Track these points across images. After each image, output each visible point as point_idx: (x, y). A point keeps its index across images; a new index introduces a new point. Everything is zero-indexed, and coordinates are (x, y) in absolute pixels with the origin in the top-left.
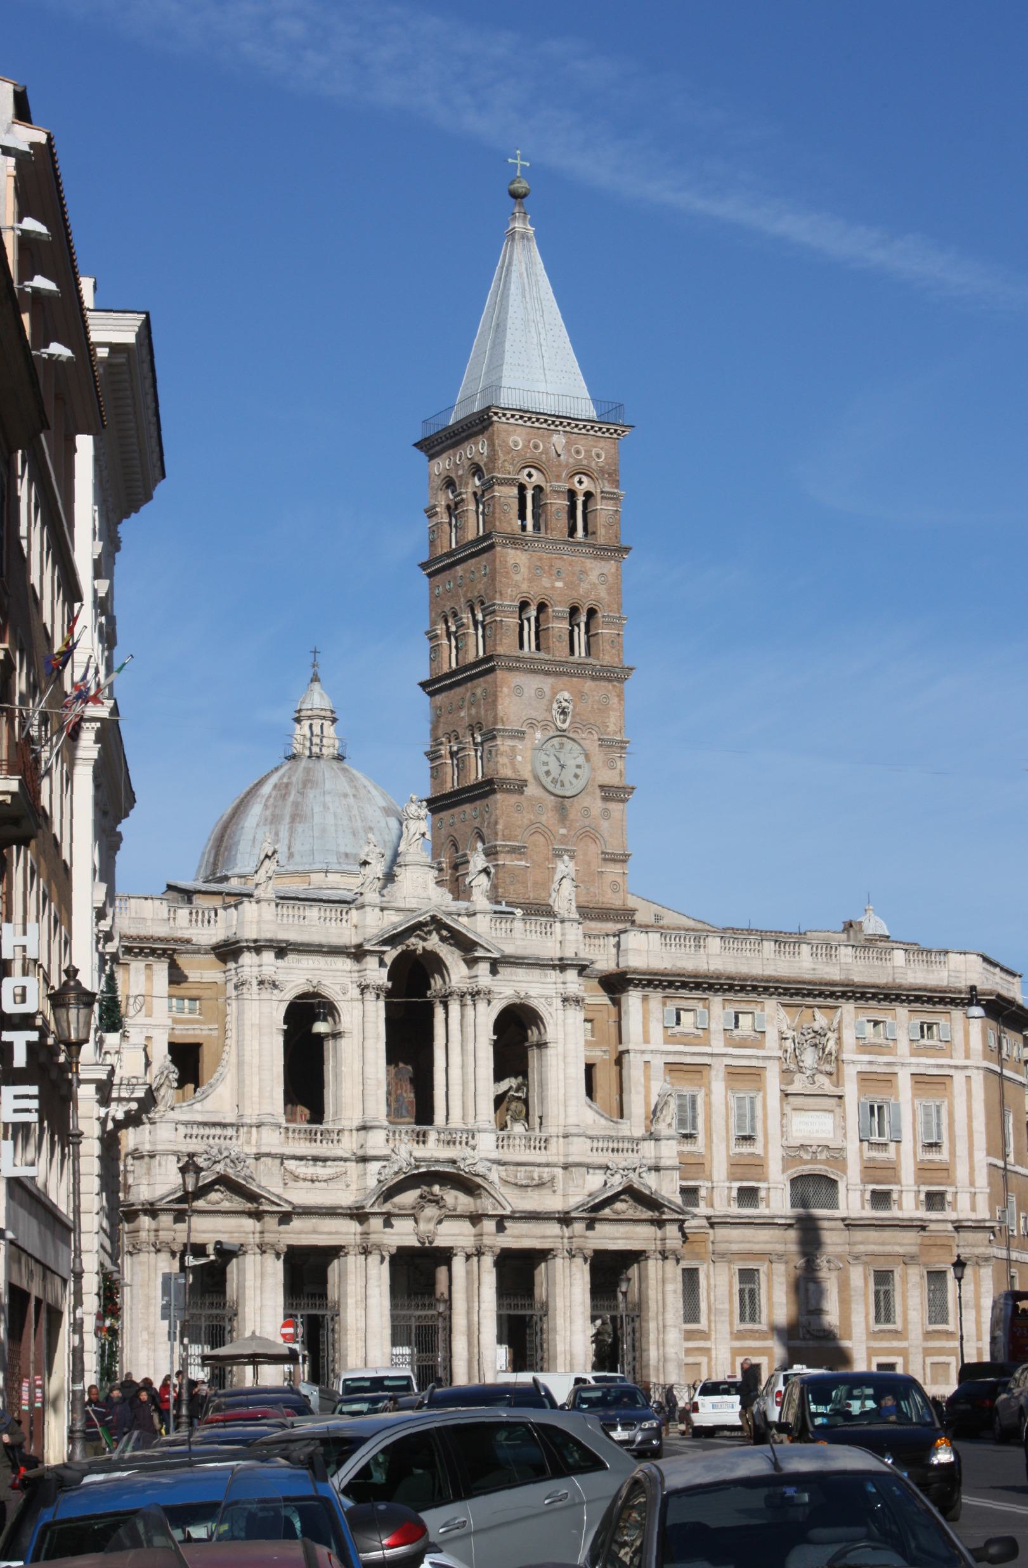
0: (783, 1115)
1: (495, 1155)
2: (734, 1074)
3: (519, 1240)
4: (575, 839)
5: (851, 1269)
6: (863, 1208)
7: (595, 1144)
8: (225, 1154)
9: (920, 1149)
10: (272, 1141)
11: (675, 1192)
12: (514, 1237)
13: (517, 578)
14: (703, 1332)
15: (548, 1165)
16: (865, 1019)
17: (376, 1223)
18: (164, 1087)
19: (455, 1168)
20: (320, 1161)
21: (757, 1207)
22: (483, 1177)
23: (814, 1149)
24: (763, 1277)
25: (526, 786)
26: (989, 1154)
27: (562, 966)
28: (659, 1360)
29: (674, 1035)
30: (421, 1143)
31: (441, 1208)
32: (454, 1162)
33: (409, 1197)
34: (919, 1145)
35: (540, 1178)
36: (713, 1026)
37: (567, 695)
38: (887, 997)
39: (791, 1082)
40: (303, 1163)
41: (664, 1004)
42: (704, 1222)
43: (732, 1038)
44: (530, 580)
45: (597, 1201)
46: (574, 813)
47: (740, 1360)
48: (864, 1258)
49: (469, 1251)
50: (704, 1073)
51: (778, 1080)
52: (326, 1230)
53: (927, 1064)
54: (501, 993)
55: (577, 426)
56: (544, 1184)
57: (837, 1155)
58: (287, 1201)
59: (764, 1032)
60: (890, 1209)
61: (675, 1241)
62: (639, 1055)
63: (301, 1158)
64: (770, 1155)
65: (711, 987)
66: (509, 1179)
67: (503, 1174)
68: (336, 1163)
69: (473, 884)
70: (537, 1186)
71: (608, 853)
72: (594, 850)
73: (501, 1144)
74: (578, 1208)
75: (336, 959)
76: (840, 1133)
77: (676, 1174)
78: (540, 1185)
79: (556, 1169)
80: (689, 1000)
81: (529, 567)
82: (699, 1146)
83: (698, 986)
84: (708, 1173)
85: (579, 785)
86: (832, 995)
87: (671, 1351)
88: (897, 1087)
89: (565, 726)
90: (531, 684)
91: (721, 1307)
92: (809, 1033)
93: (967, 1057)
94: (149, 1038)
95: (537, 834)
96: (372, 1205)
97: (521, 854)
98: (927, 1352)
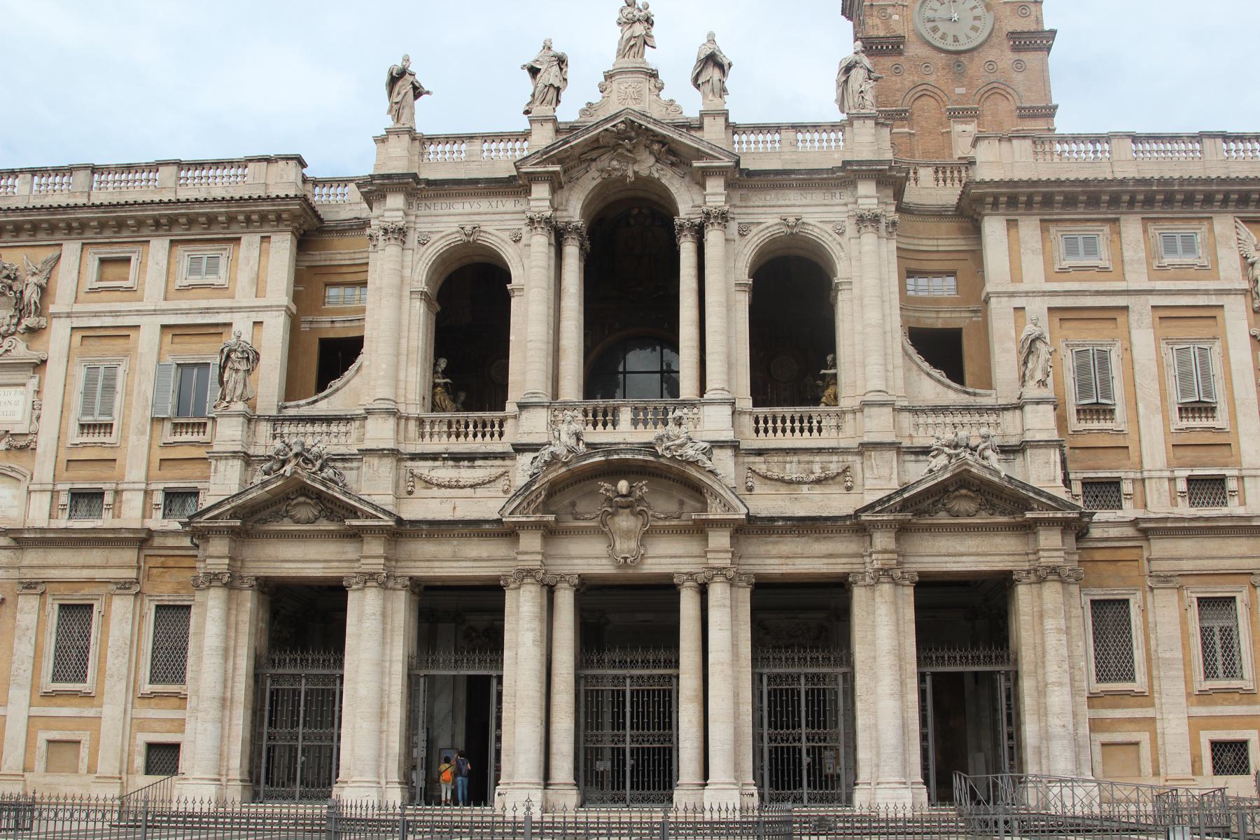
1: (728, 435)
2: (1166, 316)
3: (788, 561)
4: (977, 97)
7: (922, 419)
8: (296, 449)
10: (380, 433)
14: (1141, 694)
15: (833, 451)
17: (531, 542)
18: (227, 370)
19: (651, 454)
20: (464, 459)
21: (1224, 504)
22: (694, 463)
24: (1239, 605)
25: (903, 43)
28: (1041, 739)
29: (1063, 271)
30: (609, 427)
31: (641, 513)
32: (649, 447)
41: (1044, 230)
42: (1130, 532)
45: (906, 495)
46: (975, 67)
47: (1206, 737)
51: (1245, 324)
56: (833, 478)
58: (385, 512)
63: (434, 457)
64: (1240, 429)
65: (1115, 201)
66: (769, 473)
68: (489, 463)
69: (700, 82)
70: (818, 482)
71: (1024, 108)
72: (1003, 109)
73: (761, 424)
75: (504, 200)
77: (1055, 456)
79: (850, 458)
84: (1135, 459)
87: (1055, 723)
91: (1168, 655)
95: (924, 100)
97: (902, 119)
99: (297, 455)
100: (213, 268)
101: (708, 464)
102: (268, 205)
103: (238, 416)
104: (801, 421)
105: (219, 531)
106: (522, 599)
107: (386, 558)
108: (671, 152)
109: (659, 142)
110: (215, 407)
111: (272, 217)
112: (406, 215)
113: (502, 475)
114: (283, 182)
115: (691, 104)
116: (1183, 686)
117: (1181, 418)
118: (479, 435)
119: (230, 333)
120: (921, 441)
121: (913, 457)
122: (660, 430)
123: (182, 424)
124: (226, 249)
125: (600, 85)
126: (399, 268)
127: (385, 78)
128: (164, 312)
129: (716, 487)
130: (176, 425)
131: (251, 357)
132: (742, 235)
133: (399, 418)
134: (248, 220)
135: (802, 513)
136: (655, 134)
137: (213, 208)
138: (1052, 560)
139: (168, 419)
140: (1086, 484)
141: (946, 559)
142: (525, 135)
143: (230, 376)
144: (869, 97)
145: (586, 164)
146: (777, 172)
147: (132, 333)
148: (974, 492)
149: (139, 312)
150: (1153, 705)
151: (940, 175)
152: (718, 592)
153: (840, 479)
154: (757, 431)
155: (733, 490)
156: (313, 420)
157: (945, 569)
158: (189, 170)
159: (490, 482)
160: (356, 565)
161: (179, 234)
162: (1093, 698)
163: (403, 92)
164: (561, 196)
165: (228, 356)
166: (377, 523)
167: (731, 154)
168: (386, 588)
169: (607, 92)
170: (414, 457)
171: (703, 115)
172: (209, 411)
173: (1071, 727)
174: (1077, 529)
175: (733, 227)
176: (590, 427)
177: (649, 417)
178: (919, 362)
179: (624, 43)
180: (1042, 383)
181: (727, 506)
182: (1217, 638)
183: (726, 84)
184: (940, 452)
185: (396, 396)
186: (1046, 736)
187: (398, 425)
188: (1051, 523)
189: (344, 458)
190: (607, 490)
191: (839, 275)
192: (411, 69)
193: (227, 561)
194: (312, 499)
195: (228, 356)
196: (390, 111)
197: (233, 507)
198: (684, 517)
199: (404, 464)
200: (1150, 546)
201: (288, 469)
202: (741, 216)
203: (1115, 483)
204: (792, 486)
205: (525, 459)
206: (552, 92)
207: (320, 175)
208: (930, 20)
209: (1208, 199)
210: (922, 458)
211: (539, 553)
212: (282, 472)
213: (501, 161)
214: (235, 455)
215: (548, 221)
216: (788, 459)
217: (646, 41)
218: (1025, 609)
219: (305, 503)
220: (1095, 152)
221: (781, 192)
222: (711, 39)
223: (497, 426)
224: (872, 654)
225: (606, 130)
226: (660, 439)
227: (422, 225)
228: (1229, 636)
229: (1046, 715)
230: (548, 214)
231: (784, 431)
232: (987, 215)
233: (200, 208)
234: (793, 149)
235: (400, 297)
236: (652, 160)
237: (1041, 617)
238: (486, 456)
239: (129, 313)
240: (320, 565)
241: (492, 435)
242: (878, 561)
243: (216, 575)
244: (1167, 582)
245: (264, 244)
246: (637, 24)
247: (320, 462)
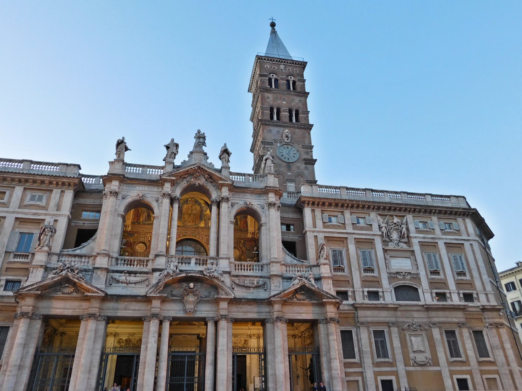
0: (385, 259)
1: (228, 270)
2: (358, 242)
5: (433, 329)
6: (433, 301)
9: (456, 275)
10: (102, 262)
11: (331, 289)
12: (243, 312)
13: (268, 100)
14: (358, 363)
15: (261, 277)
16: (418, 221)
17: (156, 303)
18: (43, 235)
19: (202, 274)
20: (132, 273)
21: (379, 300)
22: (217, 278)
23: (404, 274)
26: (489, 277)
27: (265, 191)
32: (202, 272)
33: (178, 291)
34: (455, 273)
35: (257, 283)
36: (346, 222)
37: (287, 131)
38: (426, 211)
39: (388, 245)
40: (122, 274)
41: (322, 213)
42: (351, 308)
43: (357, 227)
44: (273, 101)
45: (285, 292)
46: (294, 168)
47: (380, 378)
48: (438, 324)
49: (216, 319)
50: (345, 241)
52: (133, 308)
53: (450, 239)
54: (238, 203)
55: (287, 62)
56: (260, 286)
57: (416, 277)
58: (101, 291)
59: (371, 225)
60: (447, 301)
61: (333, 314)
62: (311, 233)
63: (121, 272)
64: (382, 276)
65: (343, 206)
66: (240, 283)
67: (237, 282)
68: (142, 275)
69: (221, 158)
71: (308, 180)
73: (237, 267)
74: (274, 296)
75: (154, 187)
76: (415, 267)
77: (331, 282)
78: (258, 287)
81: (273, 98)
82: (346, 272)
83: (337, 205)
85: (295, 159)
86: (400, 210)
87: (334, 373)
88: (439, 248)
89: (288, 141)
90: (275, 130)
92: (392, 225)
93: (468, 235)
94: (56, 221)
96: (150, 293)
98: (482, 372)
99: (68, 268)
100: (40, 199)
101: (222, 279)
102: (66, 180)
103: (45, 252)
104: (250, 267)
105: (30, 296)
106: (151, 325)
107: (99, 309)
108: (211, 178)
109: (208, 174)
110: (35, 248)
111: (67, 184)
112: (119, 188)
113: (146, 280)
114: (71, 173)
115: (218, 164)
116: (371, 360)
117: (364, 272)
118: (139, 265)
119: (44, 223)
121: (286, 280)
122: (205, 267)
123: (18, 255)
124: (46, 193)
125: (188, 155)
126: (115, 205)
127: (115, 143)
128: (17, 213)
129: (224, 287)
130: (15, 255)
131: (53, 231)
132: (232, 206)
133: (109, 257)
134: (57, 184)
135: (251, 298)
136: (206, 171)
137: (44, 178)
138: (331, 316)
139: (13, 252)
140: (338, 293)
141: (297, 314)
142: (162, 168)
143: (44, 237)
144: (272, 168)
145: (182, 179)
146: (244, 188)
148: (306, 292)
149: (7, 212)
150: (362, 367)
151: (289, 195)
152: (223, 324)
153: (262, 286)
154: (235, 269)
155: (229, 288)
156: (75, 256)
157: (296, 318)
158: (35, 164)
159: (141, 282)
160: (86, 311)
161: (28, 185)
162: (344, 364)
163: (122, 148)
164: (174, 187)
165: (44, 230)
166: (97, 295)
168: (97, 320)
169: (191, 157)
170: (114, 271)
171: (222, 168)
172: (31, 250)
173: (340, 374)
174: (337, 305)
175: (230, 203)
176: (180, 264)
177: (201, 262)
178: (286, 251)
179: (196, 144)
181: (227, 294)
182: (379, 344)
183: (230, 159)
184: (296, 278)
185: (109, 249)
186: (331, 378)
187: (109, 260)
188: (331, 303)
189: (86, 271)
190: (186, 286)
191: (262, 221)
192: (125, 141)
193: (31, 308)
194: (71, 285)
195: (44, 230)
196: (116, 154)
197: (38, 287)
198: (211, 297)
199: (109, 274)
200: (357, 312)
201: (64, 273)
202: (232, 200)
204: (247, 289)
205: (157, 274)
206: (173, 155)
207: (84, 173)
208: (281, 152)
209: (369, 207)
210: (289, 280)
211: (159, 308)
212: (61, 274)
213: (156, 174)
214: (41, 266)
215: (169, 195)
216: (246, 279)
217: (204, 144)
218: (323, 333)
219: (68, 287)
220: (336, 192)
221: (245, 194)
222: (225, 144)
223: (145, 262)
224: (274, 347)
225: (191, 168)
226: (206, 269)
227: (124, 192)
228: (383, 343)
229: (331, 370)
230: (170, 192)
231: (244, 270)
232: (306, 207)
233: (39, 177)
234: (249, 181)
235: (114, 215)
236: (204, 180)
237: (328, 335)
238: (141, 273)
240: (71, 311)
241: (143, 266)
242: (276, 315)
243: (25, 313)
244: (364, 325)
245: (62, 193)
246: (201, 139)
247: (77, 271)
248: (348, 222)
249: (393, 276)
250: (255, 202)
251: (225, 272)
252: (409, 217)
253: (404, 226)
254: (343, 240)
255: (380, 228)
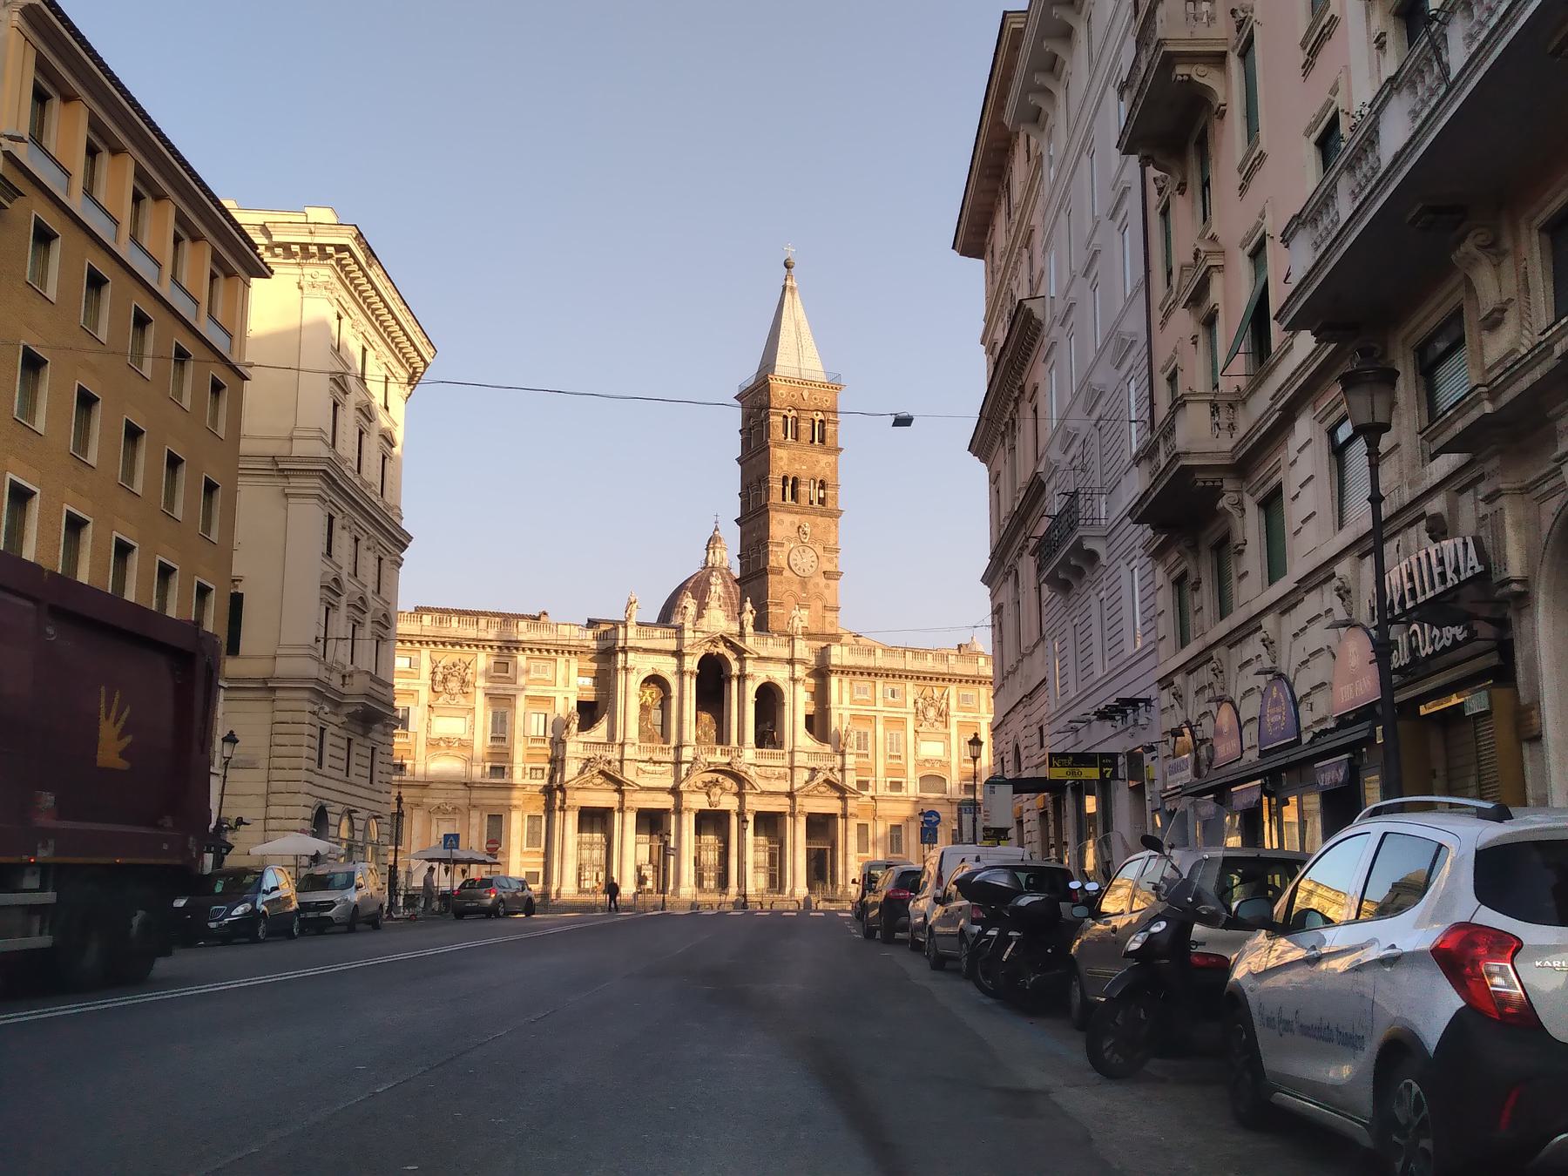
0: (915, 742)
1: (753, 762)
2: (888, 721)
8: (604, 759)
22: (746, 773)
39: (921, 725)
41: (851, 683)
58: (637, 785)
65: (876, 675)
67: (759, 772)
70: (777, 778)
80: (864, 682)
82: (870, 760)
83: (869, 674)
86: (944, 680)
94: (566, 698)
100: (545, 671)
120: (812, 764)
134: (563, 652)
140: (859, 783)
147: (512, 698)
167: (757, 653)
170: (639, 761)
180: (851, 747)
203: (867, 782)
228: (899, 838)
239: (511, 689)
248: (879, 695)
249: (920, 764)
250: (779, 675)
251: (751, 764)
252: (953, 689)
253: (944, 701)
254: (871, 720)
255: (915, 703)
